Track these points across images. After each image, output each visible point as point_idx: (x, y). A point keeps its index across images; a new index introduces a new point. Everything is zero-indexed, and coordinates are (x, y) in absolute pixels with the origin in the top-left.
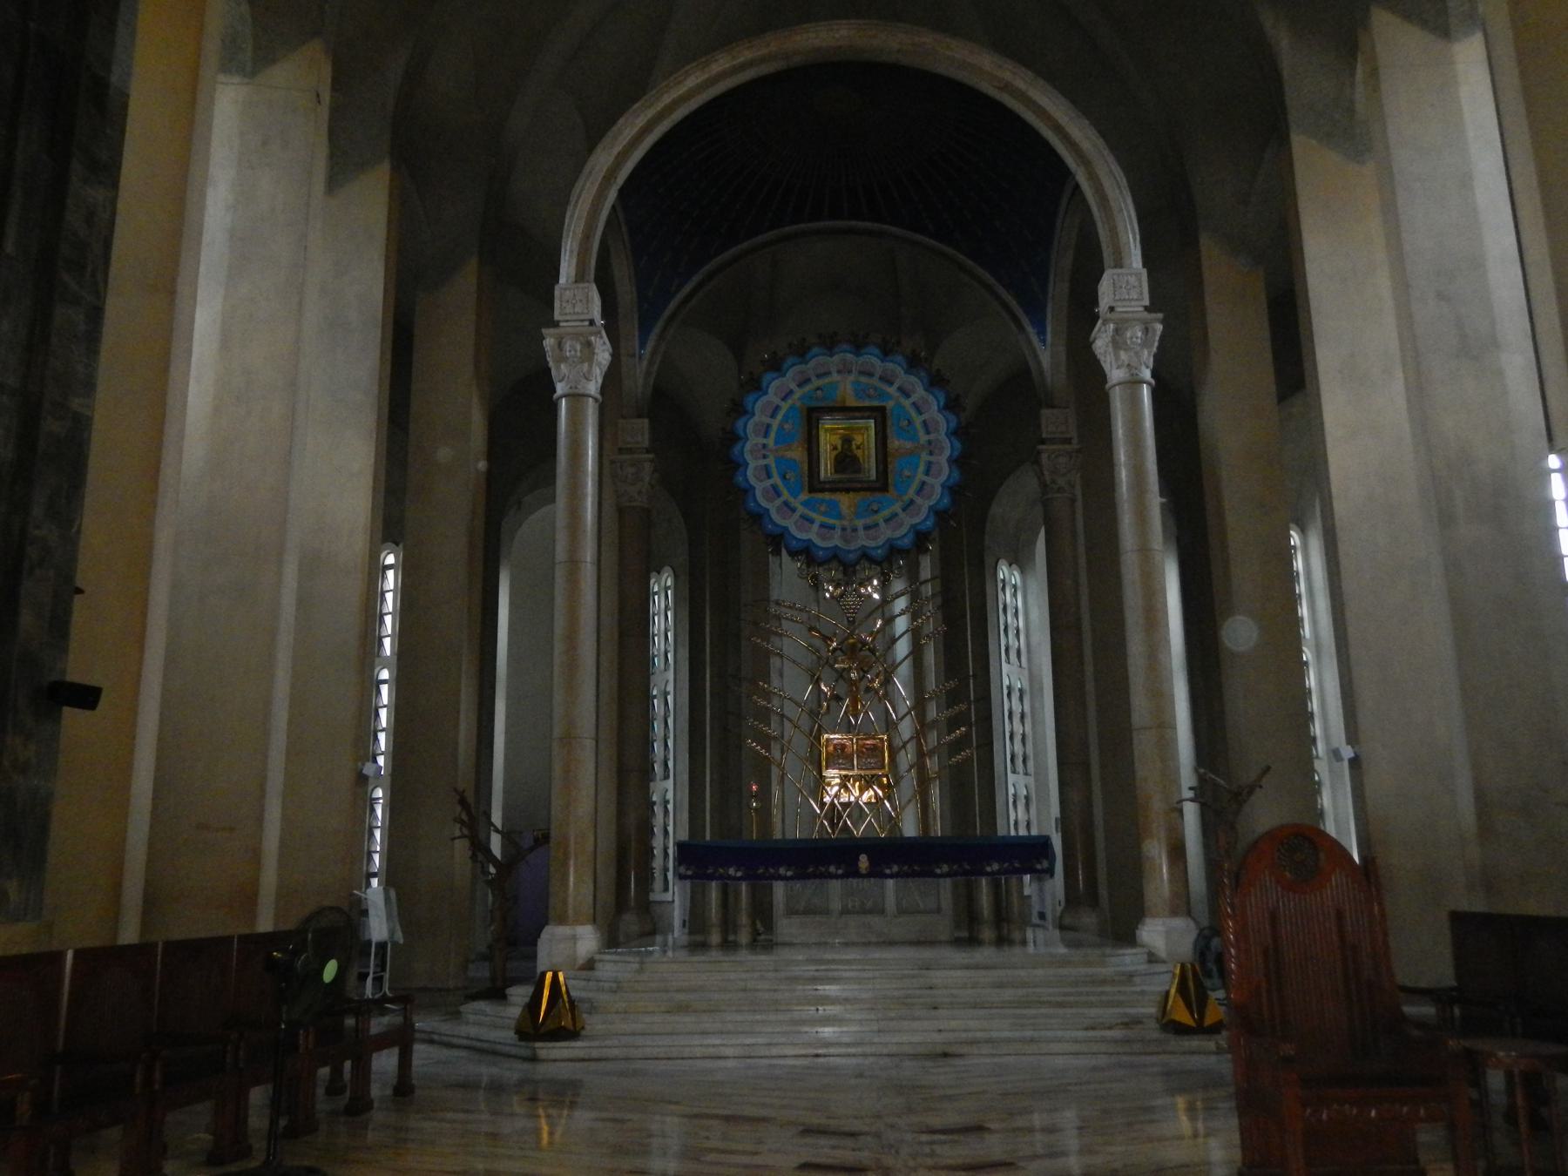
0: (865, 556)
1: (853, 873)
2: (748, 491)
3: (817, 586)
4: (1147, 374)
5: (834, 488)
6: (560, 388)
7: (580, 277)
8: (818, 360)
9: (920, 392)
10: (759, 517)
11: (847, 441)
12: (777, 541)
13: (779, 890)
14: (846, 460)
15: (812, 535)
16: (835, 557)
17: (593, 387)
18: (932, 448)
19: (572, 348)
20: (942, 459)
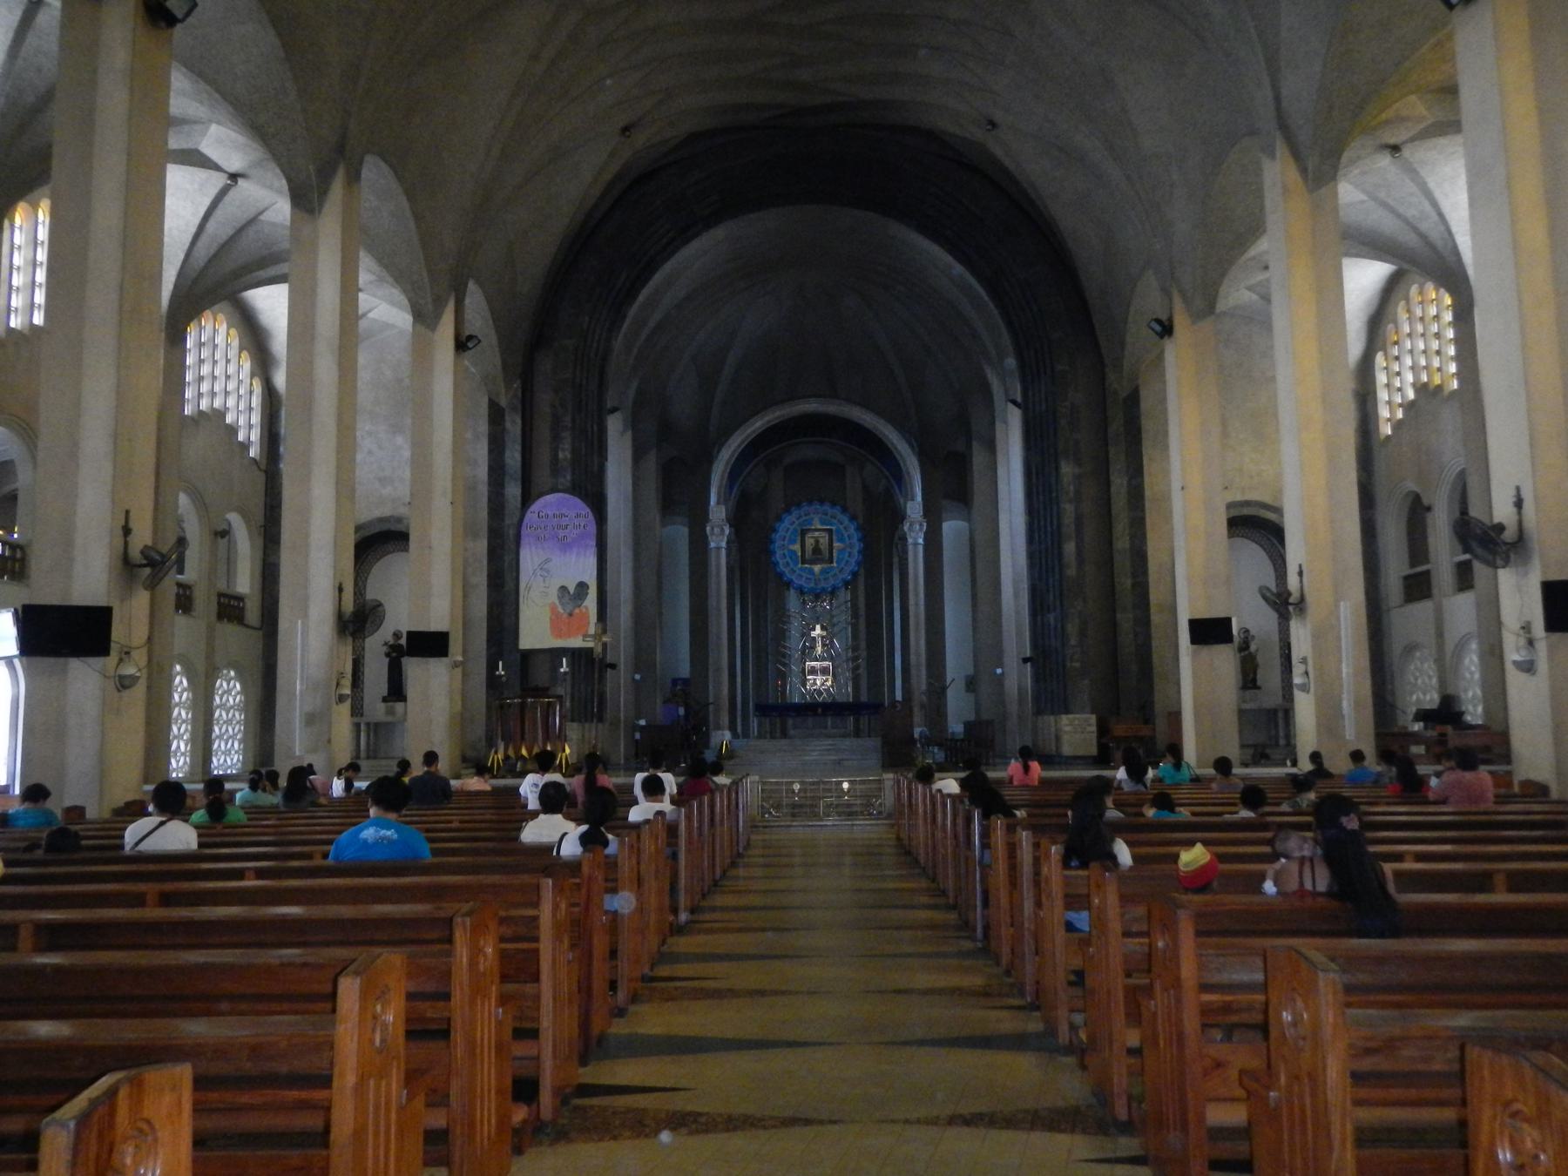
0: (823, 589)
1: (816, 714)
2: (776, 564)
3: (804, 603)
4: (921, 541)
5: (813, 562)
6: (713, 545)
7: (718, 503)
8: (805, 508)
9: (846, 522)
10: (781, 575)
11: (817, 542)
12: (789, 584)
13: (790, 722)
14: (816, 550)
15: (802, 582)
16: (811, 591)
17: (724, 544)
18: (851, 546)
19: (716, 530)
20: (855, 551)
